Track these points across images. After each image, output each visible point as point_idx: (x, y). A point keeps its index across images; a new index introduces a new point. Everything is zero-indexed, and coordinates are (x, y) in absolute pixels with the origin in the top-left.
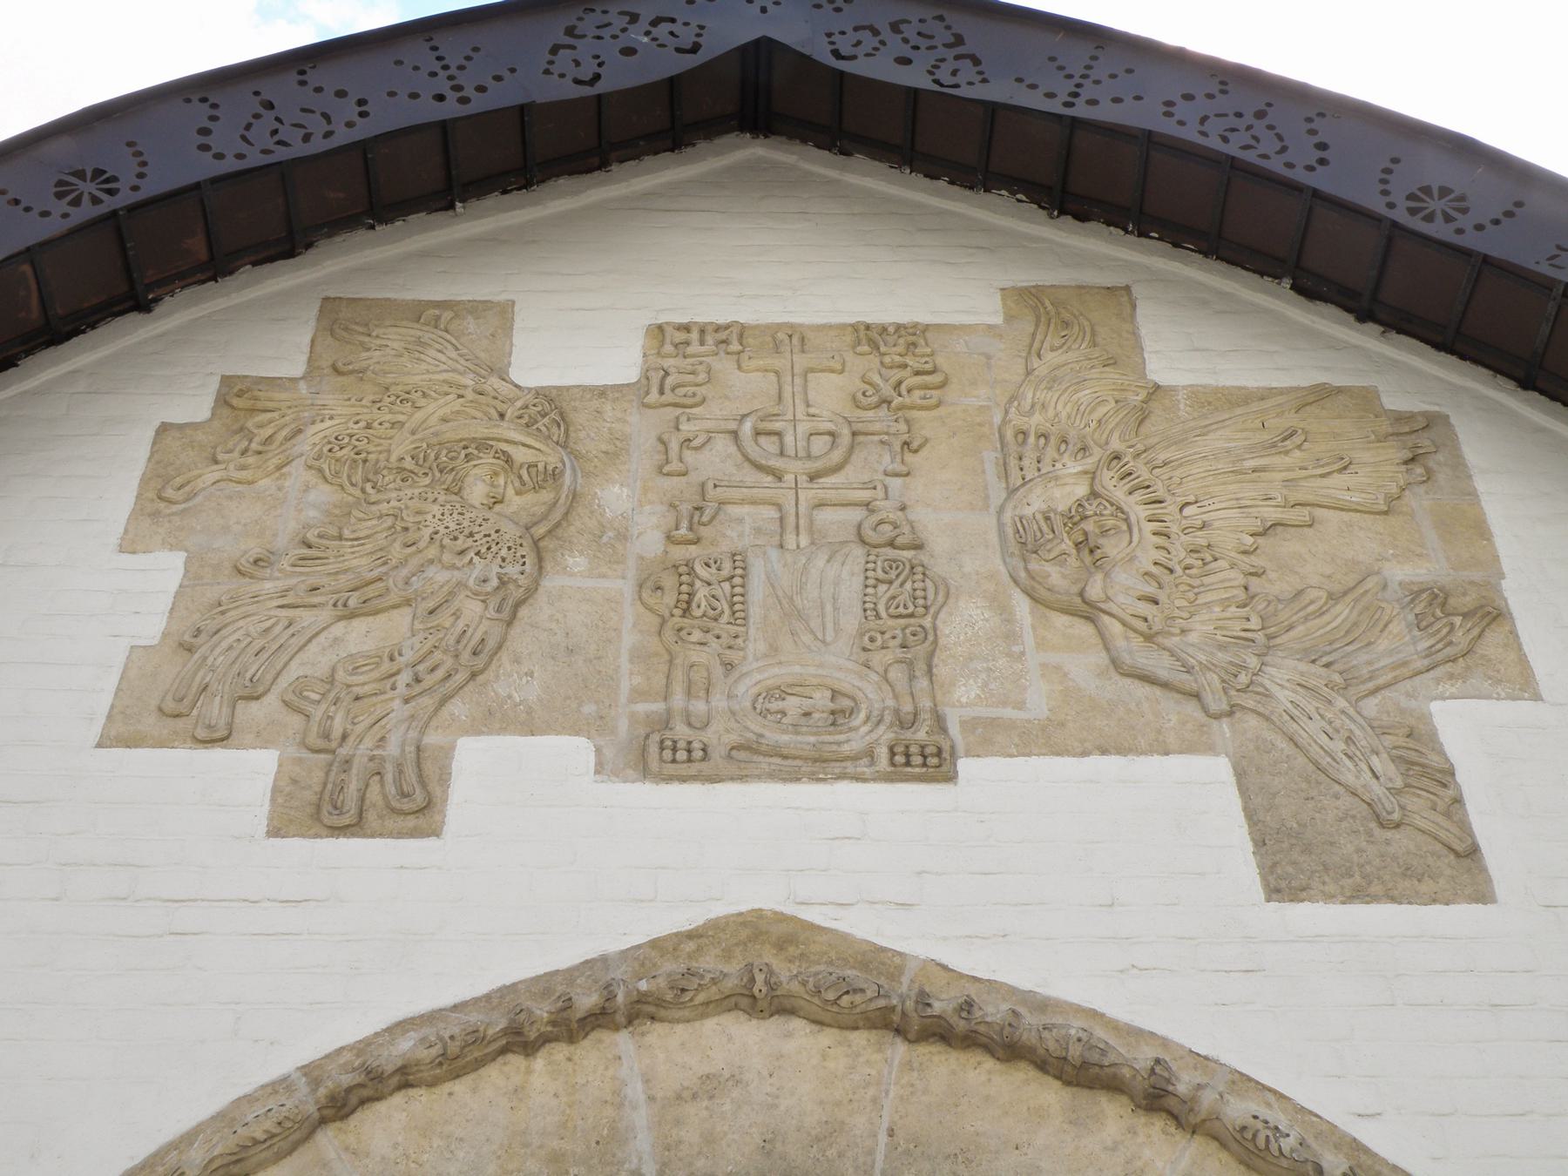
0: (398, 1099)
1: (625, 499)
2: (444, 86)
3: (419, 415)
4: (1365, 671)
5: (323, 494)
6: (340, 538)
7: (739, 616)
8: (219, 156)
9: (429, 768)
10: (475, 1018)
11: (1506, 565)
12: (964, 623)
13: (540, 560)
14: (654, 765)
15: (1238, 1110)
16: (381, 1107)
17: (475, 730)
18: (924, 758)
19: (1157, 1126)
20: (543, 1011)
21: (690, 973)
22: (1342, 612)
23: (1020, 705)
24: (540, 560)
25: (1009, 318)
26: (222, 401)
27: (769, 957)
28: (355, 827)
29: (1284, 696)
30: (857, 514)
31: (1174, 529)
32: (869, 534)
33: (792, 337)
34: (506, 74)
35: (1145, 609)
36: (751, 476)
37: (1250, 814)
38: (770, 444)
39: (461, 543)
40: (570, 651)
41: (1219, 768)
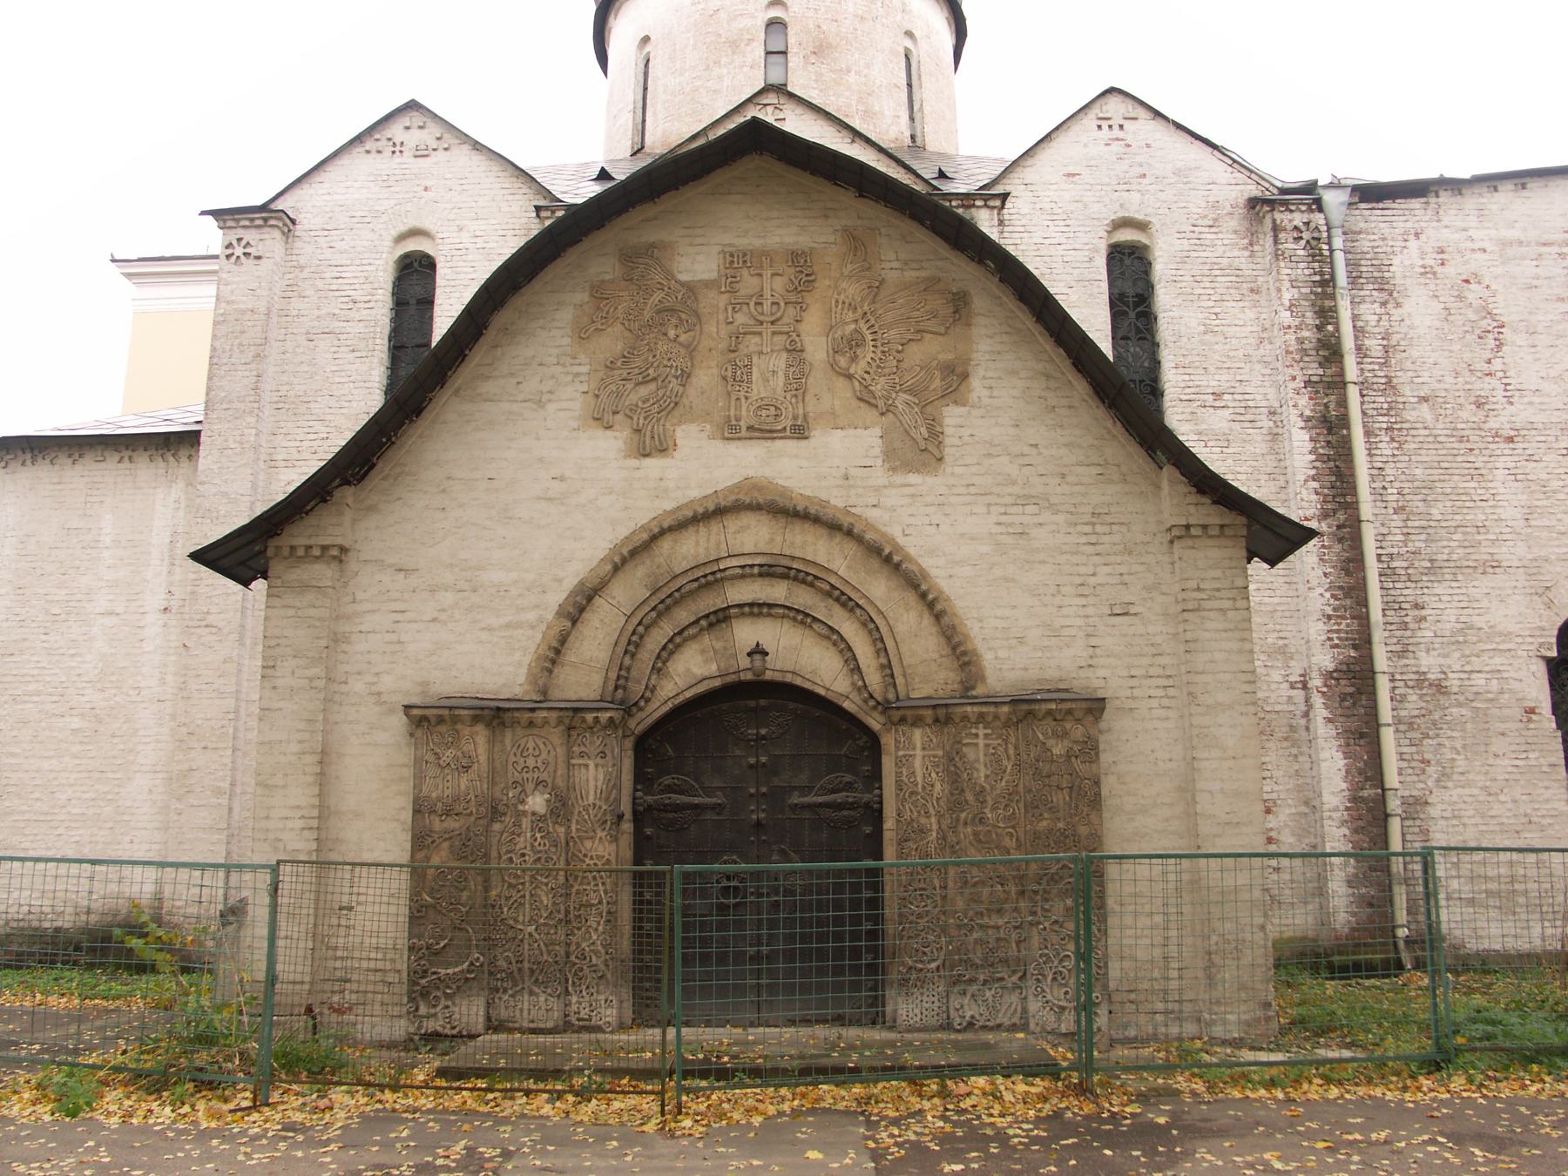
7: (750, 382)
18: (800, 432)
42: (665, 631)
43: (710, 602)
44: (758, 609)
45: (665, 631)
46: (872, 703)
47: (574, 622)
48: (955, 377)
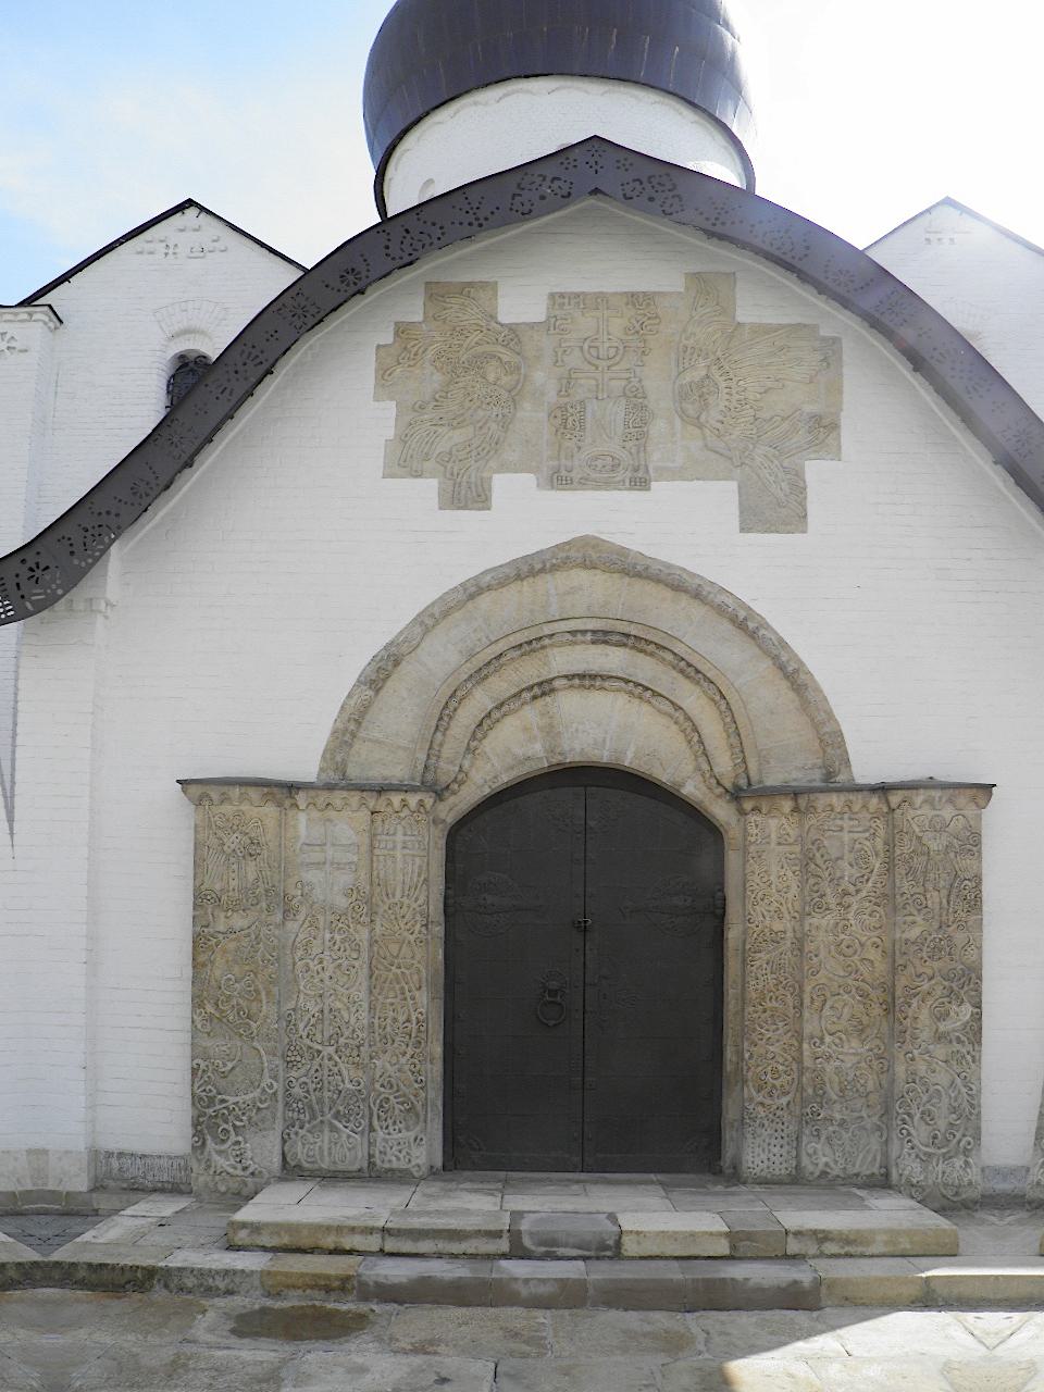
0: (487, 593)
1: (542, 377)
2: (471, 217)
3: (468, 340)
4: (786, 450)
5: (438, 377)
6: (447, 398)
7: (582, 428)
8: (393, 259)
9: (486, 486)
10: (507, 570)
11: (845, 407)
12: (658, 428)
13: (515, 405)
14: (555, 484)
15: (720, 598)
16: (483, 596)
17: (498, 472)
18: (641, 483)
19: (696, 603)
20: (525, 569)
21: (568, 558)
22: (785, 426)
23: (674, 461)
24: (515, 405)
25: (687, 289)
26: (396, 334)
27: (591, 552)
28: (465, 508)
29: (759, 460)
30: (624, 383)
31: (734, 391)
32: (628, 393)
33: (600, 300)
34: (495, 211)
35: (719, 425)
36: (587, 367)
37: (740, 504)
38: (593, 351)
39: (489, 400)
40: (527, 441)
41: (733, 486)
42: (480, 701)
43: (529, 671)
44: (587, 680)
45: (480, 701)
46: (721, 790)
47: (377, 691)
48: (823, 430)
